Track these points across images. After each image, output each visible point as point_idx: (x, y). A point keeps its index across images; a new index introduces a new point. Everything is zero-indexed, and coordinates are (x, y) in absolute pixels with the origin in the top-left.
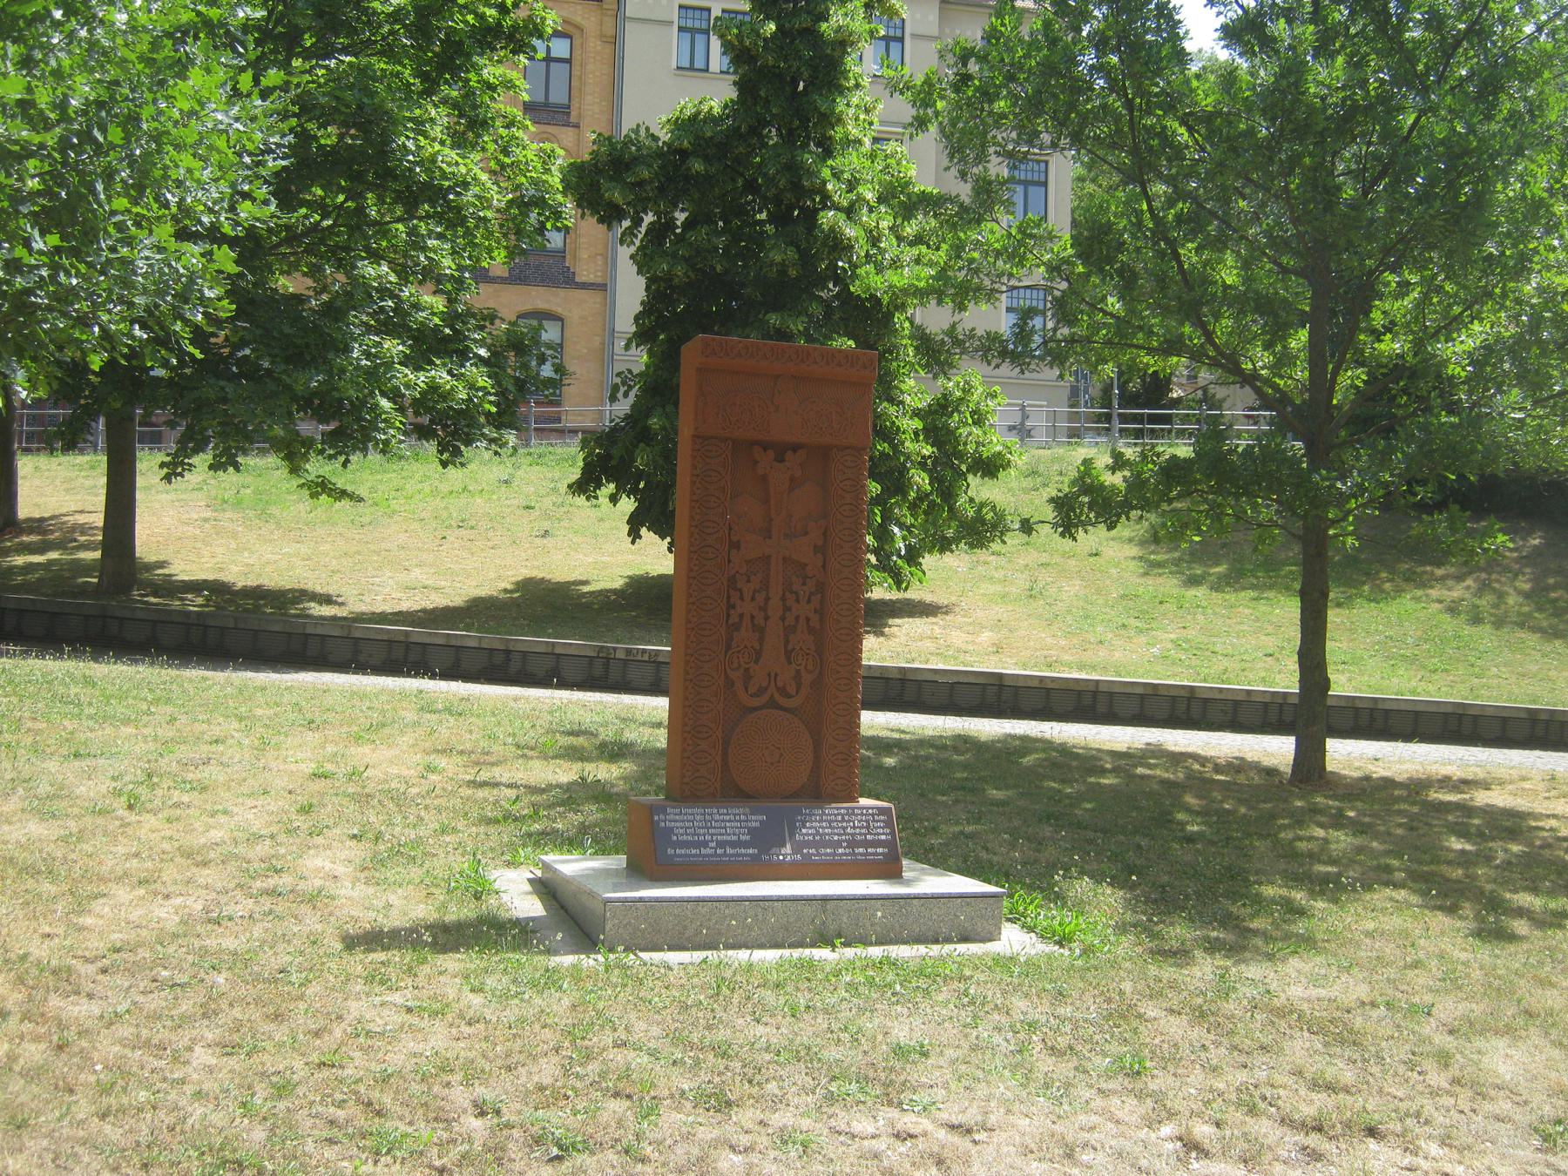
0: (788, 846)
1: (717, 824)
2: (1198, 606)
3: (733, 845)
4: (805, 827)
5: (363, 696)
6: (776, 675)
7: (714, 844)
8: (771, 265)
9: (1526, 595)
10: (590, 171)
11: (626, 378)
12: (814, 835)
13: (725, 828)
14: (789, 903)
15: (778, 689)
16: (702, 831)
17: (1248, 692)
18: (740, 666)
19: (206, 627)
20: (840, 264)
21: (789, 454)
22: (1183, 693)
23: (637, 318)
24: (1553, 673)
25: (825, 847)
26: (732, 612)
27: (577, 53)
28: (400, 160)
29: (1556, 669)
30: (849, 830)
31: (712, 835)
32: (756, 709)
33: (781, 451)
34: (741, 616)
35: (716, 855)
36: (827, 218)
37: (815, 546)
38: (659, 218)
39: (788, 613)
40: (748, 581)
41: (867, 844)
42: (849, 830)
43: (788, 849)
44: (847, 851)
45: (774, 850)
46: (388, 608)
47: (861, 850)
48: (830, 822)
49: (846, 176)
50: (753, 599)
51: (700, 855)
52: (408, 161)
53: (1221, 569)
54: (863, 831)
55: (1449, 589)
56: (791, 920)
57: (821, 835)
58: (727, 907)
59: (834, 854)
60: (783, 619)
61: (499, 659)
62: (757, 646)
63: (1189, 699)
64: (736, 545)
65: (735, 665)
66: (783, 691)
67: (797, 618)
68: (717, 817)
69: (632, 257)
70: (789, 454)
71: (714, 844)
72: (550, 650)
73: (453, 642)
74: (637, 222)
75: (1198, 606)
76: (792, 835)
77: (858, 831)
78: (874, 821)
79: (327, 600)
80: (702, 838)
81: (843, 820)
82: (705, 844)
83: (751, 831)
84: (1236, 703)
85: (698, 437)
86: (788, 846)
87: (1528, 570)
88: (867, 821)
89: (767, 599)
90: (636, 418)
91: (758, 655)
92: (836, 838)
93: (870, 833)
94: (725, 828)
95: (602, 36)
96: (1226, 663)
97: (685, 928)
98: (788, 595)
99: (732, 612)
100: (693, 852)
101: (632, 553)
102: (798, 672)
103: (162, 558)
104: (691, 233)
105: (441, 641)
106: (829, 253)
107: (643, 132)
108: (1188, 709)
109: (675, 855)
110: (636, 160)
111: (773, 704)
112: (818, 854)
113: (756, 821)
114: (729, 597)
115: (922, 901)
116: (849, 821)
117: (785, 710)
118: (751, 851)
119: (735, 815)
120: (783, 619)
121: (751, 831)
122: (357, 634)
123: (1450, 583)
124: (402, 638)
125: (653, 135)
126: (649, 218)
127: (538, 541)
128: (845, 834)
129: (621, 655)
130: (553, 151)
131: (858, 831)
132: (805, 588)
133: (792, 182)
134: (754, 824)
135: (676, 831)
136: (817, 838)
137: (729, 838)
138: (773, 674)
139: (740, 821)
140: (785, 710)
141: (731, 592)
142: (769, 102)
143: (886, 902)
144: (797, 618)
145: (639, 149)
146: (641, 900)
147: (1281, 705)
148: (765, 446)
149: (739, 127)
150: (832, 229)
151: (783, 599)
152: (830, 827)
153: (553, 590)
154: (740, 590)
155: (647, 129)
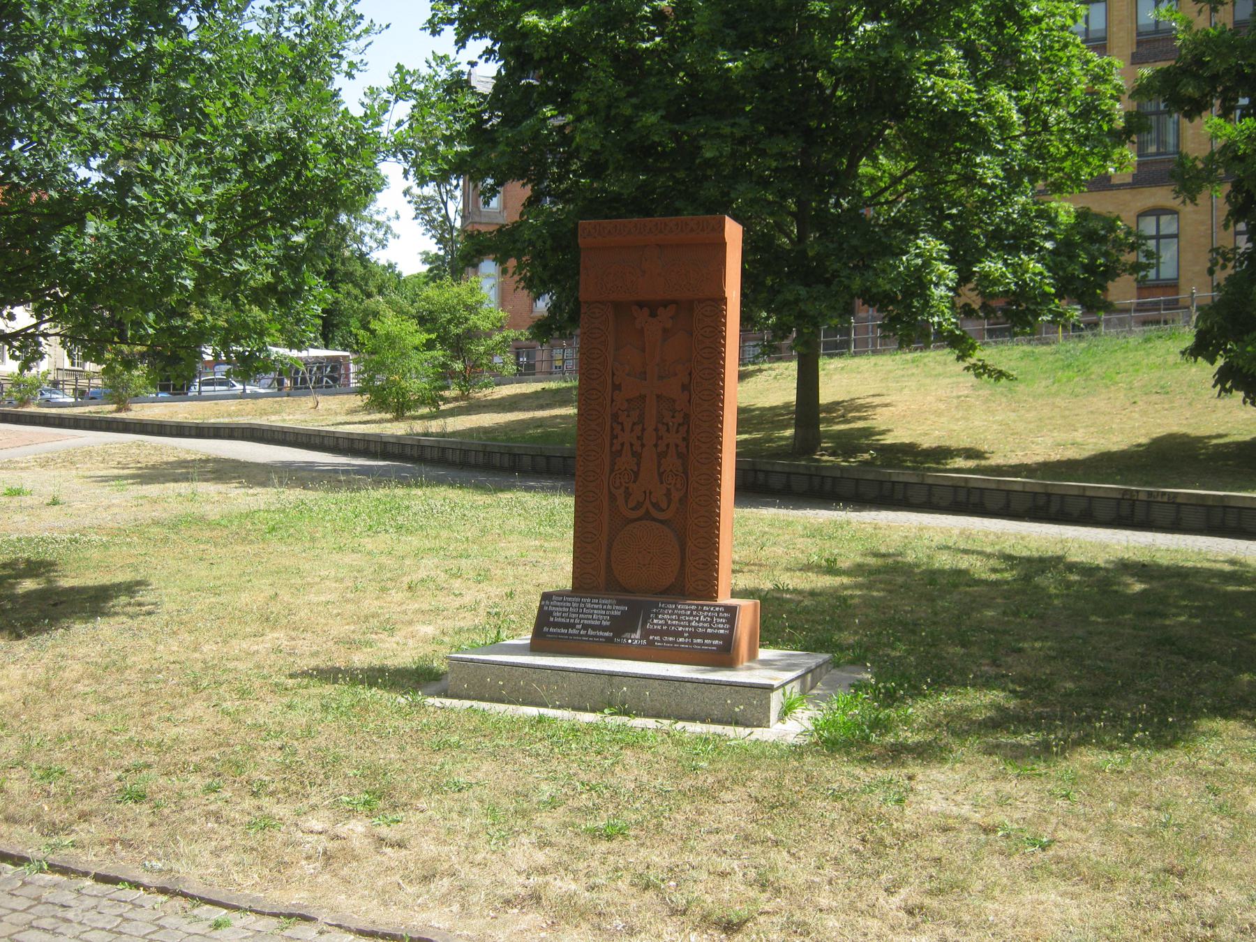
0: (639, 632)
1: (588, 611)
3: (594, 628)
4: (657, 618)
5: (789, 524)
6: (650, 493)
12: (662, 625)
13: (593, 614)
14: (583, 675)
15: (652, 503)
16: (574, 615)
19: (823, 477)
28: (920, 98)
30: (693, 624)
32: (635, 520)
33: (653, 308)
35: (579, 635)
39: (660, 442)
40: (628, 416)
41: (705, 636)
42: (693, 624)
43: (638, 635)
45: (627, 635)
46: (1013, 461)
47: (699, 641)
48: (679, 615)
51: (567, 634)
52: (927, 97)
54: (705, 625)
57: (668, 626)
58: (534, 673)
59: (675, 642)
60: (656, 446)
61: (1041, 501)
62: (635, 469)
64: (616, 387)
66: (656, 506)
67: (668, 446)
68: (589, 605)
72: (1081, 493)
73: (1003, 487)
77: (701, 624)
78: (718, 617)
79: (970, 453)
80: (572, 621)
81: (691, 615)
82: (573, 626)
86: (639, 632)
89: (643, 430)
92: (680, 629)
93: (711, 627)
98: (660, 426)
99: (615, 441)
100: (563, 631)
102: (669, 490)
103: (890, 427)
105: (993, 486)
109: (549, 633)
111: (647, 516)
112: (662, 641)
113: (618, 610)
115: (695, 685)
116: (696, 616)
117: (661, 522)
118: (607, 634)
122: (930, 481)
124: (963, 484)
128: (689, 626)
129: (1142, 497)
131: (701, 624)
134: (617, 613)
135: (554, 614)
136: (665, 628)
137: (593, 623)
139: (606, 610)
140: (661, 522)
141: (615, 425)
143: (663, 683)
144: (668, 446)
146: (472, 661)
148: (640, 305)
151: (656, 430)
152: (679, 620)
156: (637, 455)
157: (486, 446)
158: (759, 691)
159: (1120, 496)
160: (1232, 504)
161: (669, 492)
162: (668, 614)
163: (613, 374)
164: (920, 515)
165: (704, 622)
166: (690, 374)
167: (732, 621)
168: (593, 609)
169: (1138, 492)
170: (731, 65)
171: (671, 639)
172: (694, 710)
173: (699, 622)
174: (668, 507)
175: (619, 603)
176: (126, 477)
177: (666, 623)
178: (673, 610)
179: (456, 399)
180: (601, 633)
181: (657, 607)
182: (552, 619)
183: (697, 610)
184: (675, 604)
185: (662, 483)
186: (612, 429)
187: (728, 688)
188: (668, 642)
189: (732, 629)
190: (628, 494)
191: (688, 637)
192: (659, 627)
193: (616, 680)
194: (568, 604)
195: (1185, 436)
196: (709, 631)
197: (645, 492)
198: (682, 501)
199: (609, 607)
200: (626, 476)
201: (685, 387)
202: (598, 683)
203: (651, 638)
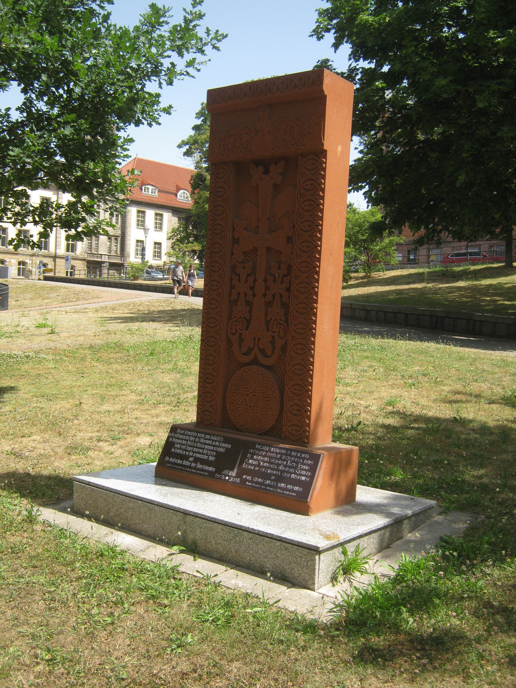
0: (235, 471)
3: (203, 462)
4: (252, 458)
6: (259, 339)
7: (191, 459)
12: (255, 466)
15: (259, 349)
16: (189, 448)
25: (258, 477)
30: (280, 468)
31: (194, 452)
32: (248, 364)
35: (190, 467)
39: (268, 291)
40: (244, 268)
42: (280, 468)
43: (233, 473)
45: (226, 472)
48: (271, 458)
51: (182, 465)
56: (166, 523)
58: (130, 502)
59: (262, 484)
62: (248, 318)
66: (262, 351)
68: (202, 440)
76: (241, 463)
80: (187, 453)
81: (280, 459)
83: (218, 455)
86: (235, 471)
89: (255, 281)
93: (295, 473)
94: (203, 449)
100: (179, 462)
109: (169, 462)
111: (255, 362)
113: (223, 447)
116: (285, 460)
117: (267, 367)
118: (211, 469)
119: (213, 441)
120: (265, 295)
121: (218, 455)
128: (277, 470)
134: (222, 450)
136: (257, 469)
138: (257, 339)
139: (214, 446)
140: (267, 367)
146: (89, 484)
148: (257, 163)
151: (265, 280)
152: (270, 463)
154: (238, 275)
156: (249, 304)
157: (351, 304)
158: (306, 551)
162: (261, 455)
163: (234, 229)
165: (290, 467)
166: (294, 227)
167: (313, 469)
170: (499, 40)
172: (250, 560)
173: (286, 466)
174: (272, 355)
175: (226, 440)
176: (116, 318)
177: (259, 463)
178: (267, 452)
179: (362, 278)
180: (206, 468)
182: (173, 450)
186: (231, 279)
187: (279, 543)
188: (257, 483)
189: (312, 477)
190: (241, 340)
191: (274, 480)
192: (252, 468)
193: (189, 519)
194: (187, 438)
196: (293, 476)
198: (284, 348)
199: (217, 443)
201: (289, 240)
202: (177, 519)
203: (244, 477)
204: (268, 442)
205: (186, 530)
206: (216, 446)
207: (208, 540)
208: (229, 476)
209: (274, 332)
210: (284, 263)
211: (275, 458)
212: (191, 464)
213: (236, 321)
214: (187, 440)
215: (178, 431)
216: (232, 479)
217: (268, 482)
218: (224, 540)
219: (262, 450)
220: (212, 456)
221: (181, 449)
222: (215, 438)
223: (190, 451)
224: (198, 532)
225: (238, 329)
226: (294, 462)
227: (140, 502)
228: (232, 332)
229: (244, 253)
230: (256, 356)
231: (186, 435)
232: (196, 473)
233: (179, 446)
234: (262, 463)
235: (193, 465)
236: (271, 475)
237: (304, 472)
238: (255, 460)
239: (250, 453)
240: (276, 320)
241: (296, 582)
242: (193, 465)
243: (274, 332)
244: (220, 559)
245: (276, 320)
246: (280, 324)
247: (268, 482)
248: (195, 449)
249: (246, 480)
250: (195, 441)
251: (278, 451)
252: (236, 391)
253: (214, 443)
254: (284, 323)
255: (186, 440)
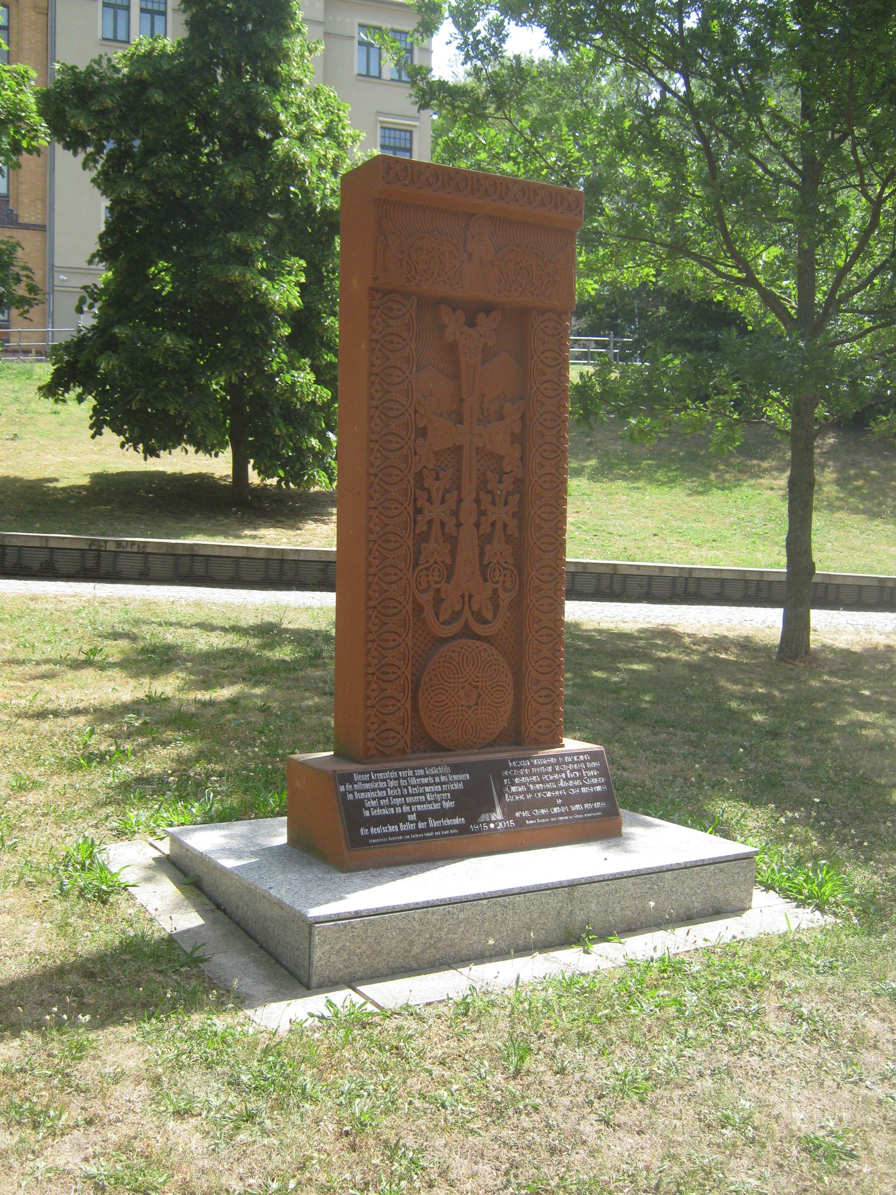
1: (415, 790)
2: (583, 494)
4: (513, 784)
6: (471, 596)
7: (413, 817)
8: (230, 189)
9: (837, 482)
10: (56, 99)
11: (92, 293)
15: (473, 612)
16: (398, 801)
17: (661, 568)
18: (429, 586)
20: (292, 189)
21: (481, 317)
22: (607, 570)
23: (101, 237)
24: (873, 547)
25: (539, 808)
26: (419, 517)
27: (14, 22)
29: (874, 543)
31: (410, 805)
34: (430, 523)
35: (418, 831)
36: (282, 145)
37: (512, 434)
38: (120, 146)
40: (437, 478)
42: (562, 784)
43: (498, 815)
44: (563, 809)
45: (484, 817)
47: (577, 807)
48: (540, 774)
49: (294, 109)
50: (443, 501)
51: (400, 833)
53: (593, 462)
54: (577, 783)
55: (775, 479)
57: (532, 792)
58: (462, 910)
60: (477, 525)
63: (612, 575)
65: (424, 585)
68: (413, 781)
69: (94, 181)
70: (481, 317)
71: (413, 817)
72: (44, 545)
74: (100, 149)
75: (583, 494)
76: (501, 796)
78: (587, 769)
80: (399, 810)
81: (554, 772)
82: (402, 818)
83: (455, 795)
84: (650, 578)
85: (377, 290)
87: (830, 463)
88: (579, 770)
89: (460, 500)
90: (101, 329)
91: (450, 571)
92: (549, 794)
93: (584, 785)
94: (424, 794)
95: (36, 7)
96: (621, 543)
97: (412, 943)
98: (482, 494)
99: (419, 517)
100: (392, 829)
101: (95, 453)
102: (495, 591)
104: (152, 159)
106: (284, 177)
107: (105, 63)
108: (611, 584)
110: (99, 90)
111: (467, 633)
112: (533, 817)
113: (458, 781)
114: (415, 499)
116: (560, 772)
117: (479, 638)
118: (457, 821)
119: (433, 776)
120: (477, 525)
121: (455, 795)
123: (775, 473)
125: (114, 67)
126: (110, 145)
127: (9, 443)
129: (111, 547)
130: (26, 72)
132: (501, 486)
133: (246, 113)
135: (368, 804)
136: (529, 796)
137: (429, 807)
139: (441, 784)
140: (479, 638)
142: (219, 38)
143: (637, 880)
145: (102, 79)
147: (686, 579)
149: (194, 62)
150: (287, 156)
151: (478, 501)
152: (542, 782)
153: (30, 487)
154: (428, 490)
155: (109, 60)
156: (453, 541)
159: (87, 547)
160: (202, 552)
161: (495, 597)
162: (525, 775)
163: (416, 412)
164: (264, 592)
165: (573, 779)
168: (422, 785)
169: (106, 542)
171: (543, 811)
174: (494, 618)
175: (456, 769)
177: (528, 788)
178: (529, 767)
180: (448, 822)
181: (508, 769)
182: (367, 813)
183: (558, 763)
184: (528, 758)
185: (485, 580)
187: (712, 867)
188: (541, 817)
190: (438, 601)
193: (578, 892)
195: (16, 480)
196: (584, 790)
197: (462, 596)
200: (436, 573)
202: (554, 901)
203: (517, 814)
204: (526, 753)
205: (571, 912)
206: (445, 783)
207: (609, 910)
208: (494, 822)
209: (497, 582)
210: (507, 474)
211: (547, 773)
212: (417, 826)
213: (427, 569)
214: (385, 789)
215: (356, 777)
216: (500, 824)
217: (556, 810)
218: (635, 899)
219: (522, 767)
220: (446, 801)
221: (382, 807)
222: (434, 771)
223: (401, 806)
224: (593, 907)
225: (432, 583)
226: (574, 770)
227: (485, 902)
228: (421, 588)
229: (436, 453)
230: (466, 622)
231: (376, 781)
232: (434, 837)
233: (374, 803)
234: (531, 786)
235: (421, 825)
236: (553, 798)
237: (595, 781)
238: (520, 785)
239: (506, 778)
240: (498, 563)
241: (729, 908)
242: (421, 825)
243: (497, 582)
244: (631, 929)
245: (498, 563)
246: (505, 569)
247: (556, 810)
248: (409, 800)
249: (523, 819)
250: (400, 787)
251: (545, 762)
252: (442, 686)
253: (437, 780)
254: (512, 568)
255: (381, 789)
